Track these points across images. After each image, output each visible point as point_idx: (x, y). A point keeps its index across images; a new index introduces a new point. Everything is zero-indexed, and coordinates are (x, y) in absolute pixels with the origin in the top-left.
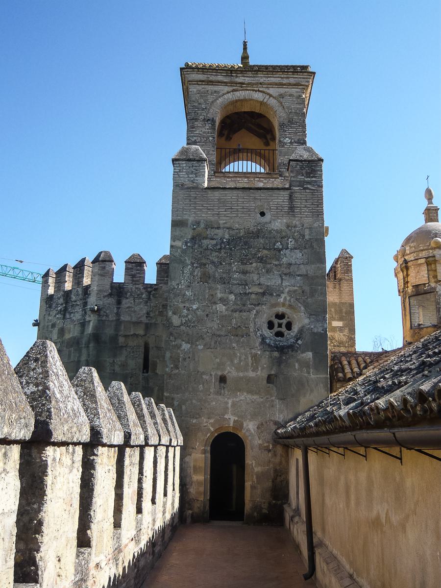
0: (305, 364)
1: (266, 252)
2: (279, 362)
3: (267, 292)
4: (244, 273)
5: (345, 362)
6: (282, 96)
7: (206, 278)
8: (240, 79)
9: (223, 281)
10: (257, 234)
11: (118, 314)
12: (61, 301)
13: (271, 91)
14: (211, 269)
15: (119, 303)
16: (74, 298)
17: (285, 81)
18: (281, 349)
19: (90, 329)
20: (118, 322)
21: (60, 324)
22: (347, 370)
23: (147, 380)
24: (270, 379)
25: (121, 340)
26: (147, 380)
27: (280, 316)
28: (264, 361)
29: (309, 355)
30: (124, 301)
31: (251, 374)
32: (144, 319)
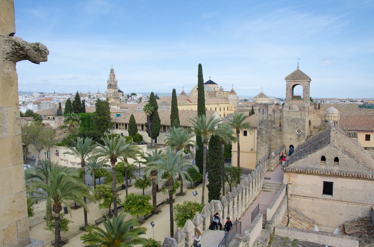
0: (302, 137)
1: (297, 121)
2: (298, 137)
3: (297, 127)
4: (294, 124)
5: (313, 132)
6: (304, 83)
7: (288, 125)
8: (296, 81)
9: (291, 125)
10: (296, 118)
11: (274, 116)
12: (262, 111)
13: (302, 82)
14: (289, 124)
15: (274, 113)
16: (265, 111)
17: (304, 80)
18: (299, 135)
19: (269, 118)
20: (274, 118)
21: (262, 116)
22: (313, 133)
23: (280, 128)
24: (297, 138)
25: (275, 121)
26: (280, 128)
27: (299, 130)
28: (297, 136)
29: (303, 136)
30: (275, 113)
31: (295, 138)
32: (280, 117)
